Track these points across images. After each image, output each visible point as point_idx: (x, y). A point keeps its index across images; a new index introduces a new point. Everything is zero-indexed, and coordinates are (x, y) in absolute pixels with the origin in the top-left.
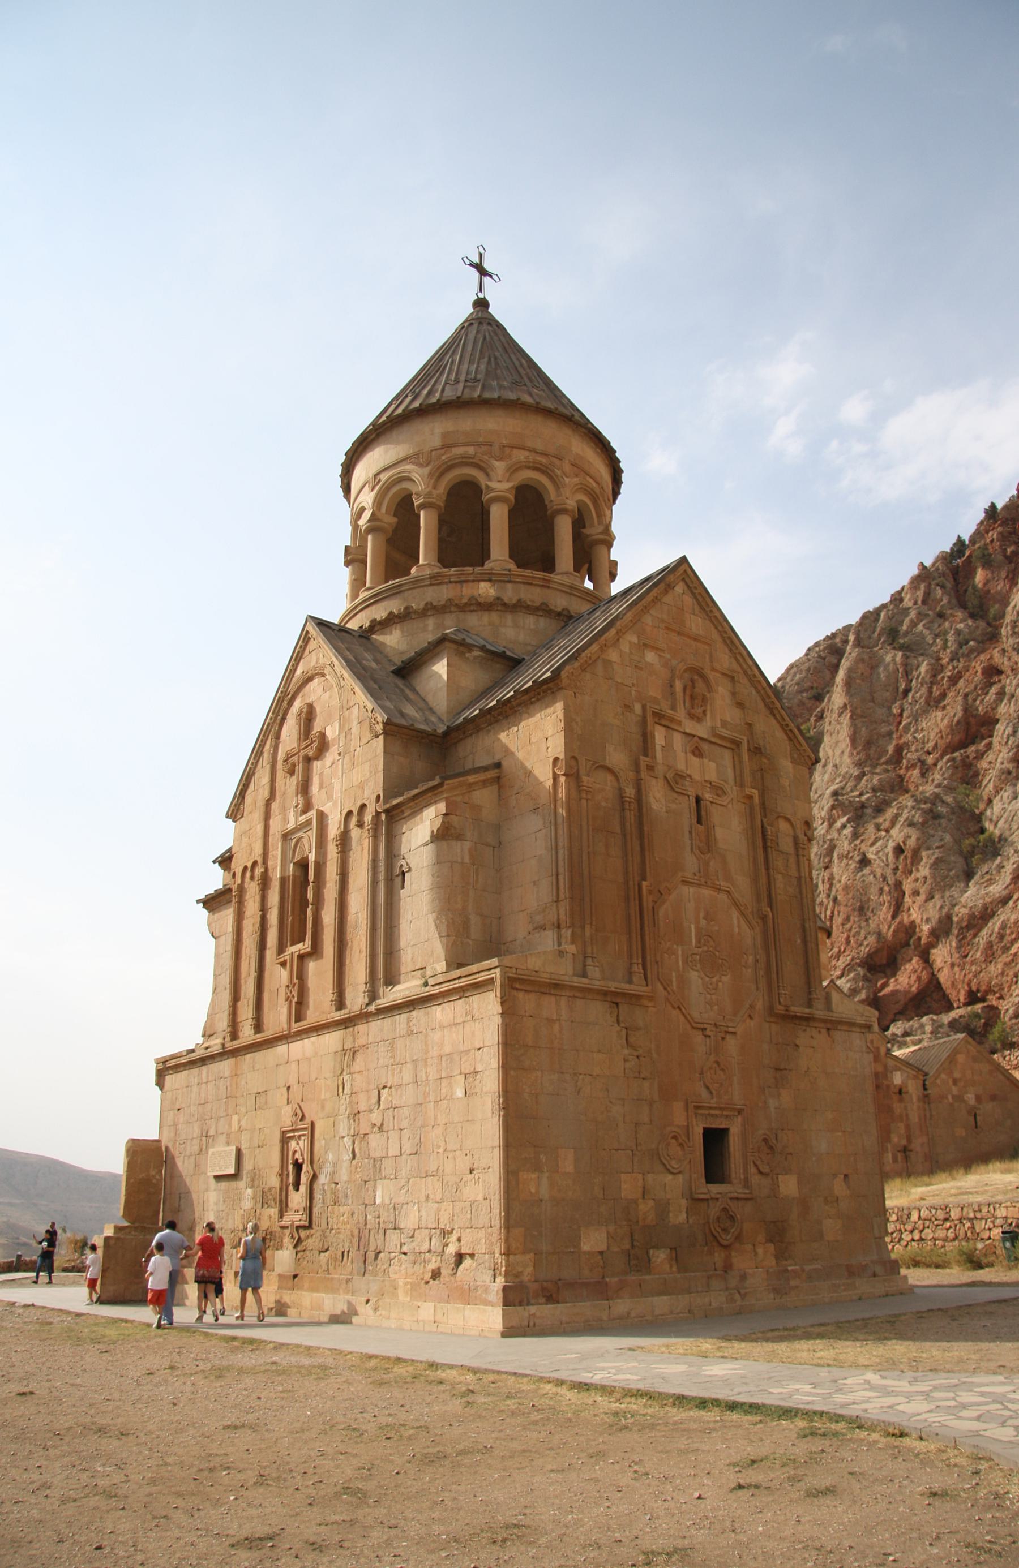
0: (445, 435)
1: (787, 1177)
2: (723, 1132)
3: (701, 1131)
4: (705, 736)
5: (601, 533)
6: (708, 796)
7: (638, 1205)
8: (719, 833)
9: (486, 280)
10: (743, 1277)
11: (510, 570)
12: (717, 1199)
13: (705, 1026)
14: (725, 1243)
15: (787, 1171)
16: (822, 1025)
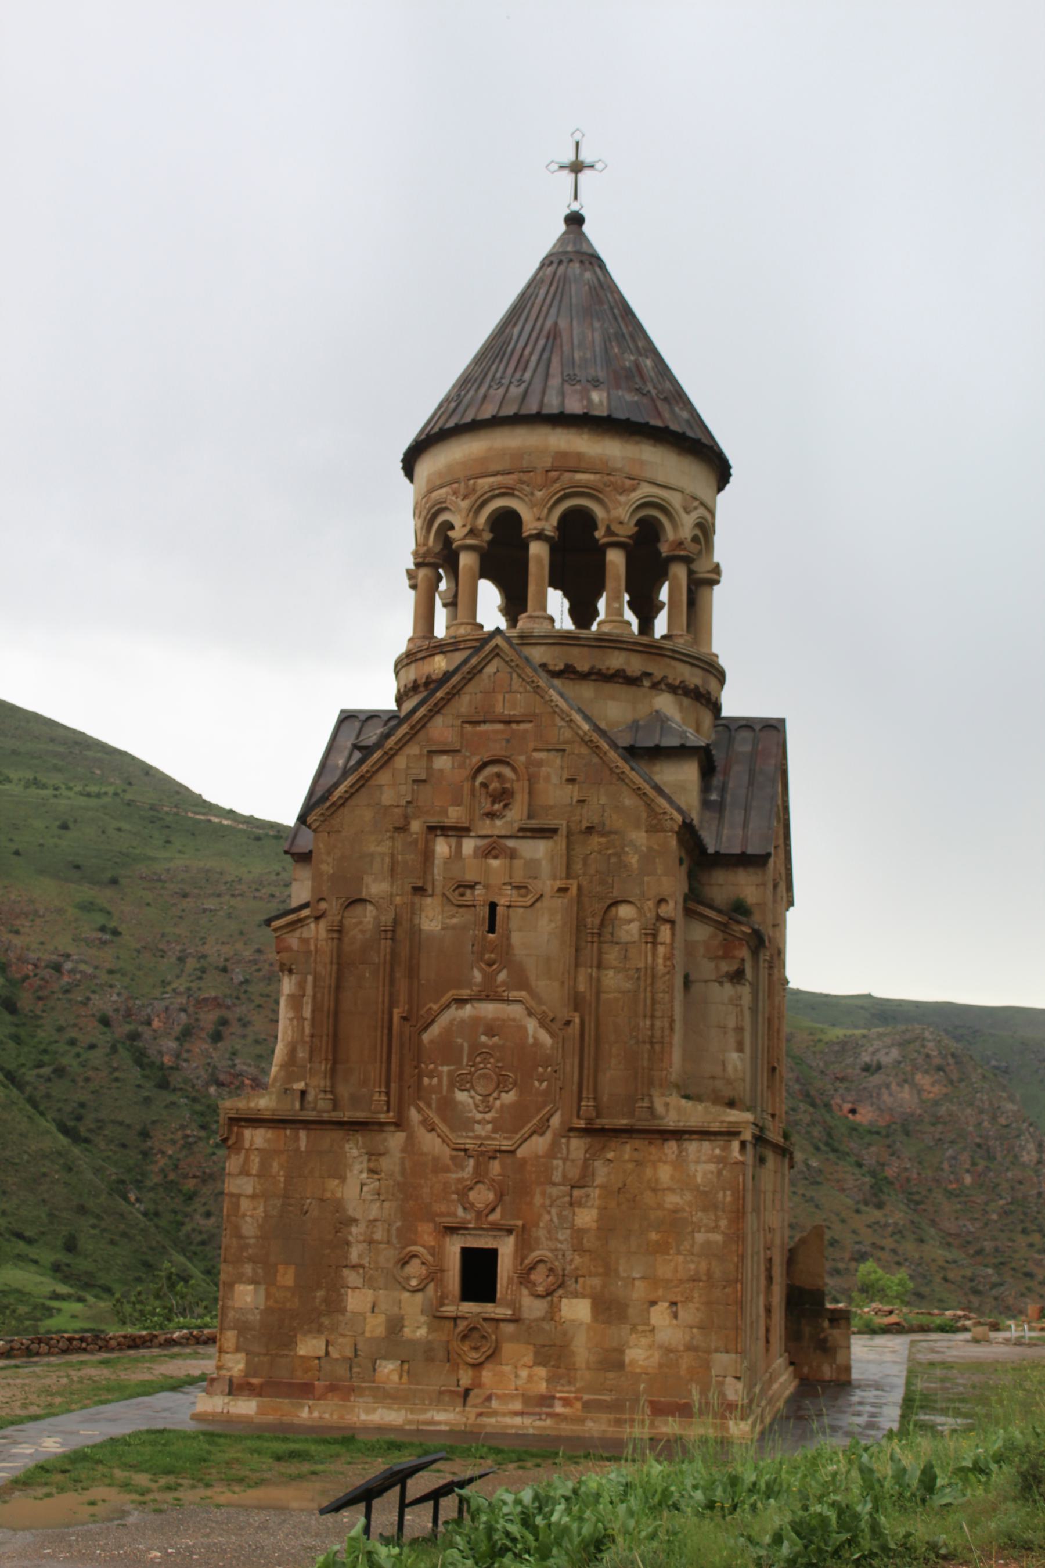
0: (429, 481)
1: (575, 1301)
2: (493, 1253)
3: (458, 1251)
4: (508, 834)
5: (604, 536)
6: (502, 901)
7: (365, 1319)
8: (516, 938)
9: (585, 176)
10: (489, 1398)
11: (455, 637)
12: (466, 1318)
13: (467, 1146)
14: (471, 1361)
15: (576, 1295)
16: (656, 1136)
